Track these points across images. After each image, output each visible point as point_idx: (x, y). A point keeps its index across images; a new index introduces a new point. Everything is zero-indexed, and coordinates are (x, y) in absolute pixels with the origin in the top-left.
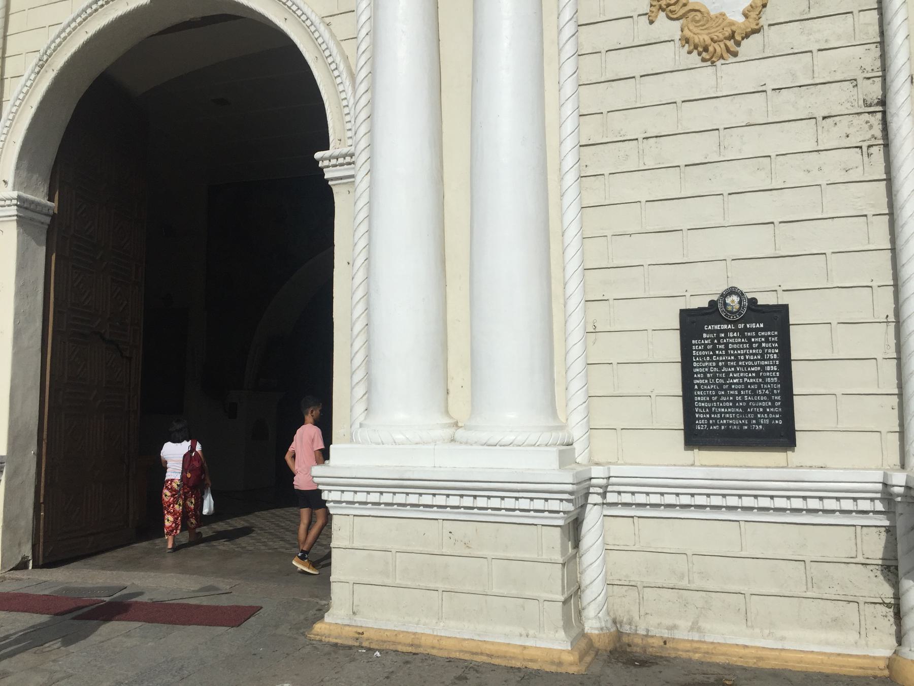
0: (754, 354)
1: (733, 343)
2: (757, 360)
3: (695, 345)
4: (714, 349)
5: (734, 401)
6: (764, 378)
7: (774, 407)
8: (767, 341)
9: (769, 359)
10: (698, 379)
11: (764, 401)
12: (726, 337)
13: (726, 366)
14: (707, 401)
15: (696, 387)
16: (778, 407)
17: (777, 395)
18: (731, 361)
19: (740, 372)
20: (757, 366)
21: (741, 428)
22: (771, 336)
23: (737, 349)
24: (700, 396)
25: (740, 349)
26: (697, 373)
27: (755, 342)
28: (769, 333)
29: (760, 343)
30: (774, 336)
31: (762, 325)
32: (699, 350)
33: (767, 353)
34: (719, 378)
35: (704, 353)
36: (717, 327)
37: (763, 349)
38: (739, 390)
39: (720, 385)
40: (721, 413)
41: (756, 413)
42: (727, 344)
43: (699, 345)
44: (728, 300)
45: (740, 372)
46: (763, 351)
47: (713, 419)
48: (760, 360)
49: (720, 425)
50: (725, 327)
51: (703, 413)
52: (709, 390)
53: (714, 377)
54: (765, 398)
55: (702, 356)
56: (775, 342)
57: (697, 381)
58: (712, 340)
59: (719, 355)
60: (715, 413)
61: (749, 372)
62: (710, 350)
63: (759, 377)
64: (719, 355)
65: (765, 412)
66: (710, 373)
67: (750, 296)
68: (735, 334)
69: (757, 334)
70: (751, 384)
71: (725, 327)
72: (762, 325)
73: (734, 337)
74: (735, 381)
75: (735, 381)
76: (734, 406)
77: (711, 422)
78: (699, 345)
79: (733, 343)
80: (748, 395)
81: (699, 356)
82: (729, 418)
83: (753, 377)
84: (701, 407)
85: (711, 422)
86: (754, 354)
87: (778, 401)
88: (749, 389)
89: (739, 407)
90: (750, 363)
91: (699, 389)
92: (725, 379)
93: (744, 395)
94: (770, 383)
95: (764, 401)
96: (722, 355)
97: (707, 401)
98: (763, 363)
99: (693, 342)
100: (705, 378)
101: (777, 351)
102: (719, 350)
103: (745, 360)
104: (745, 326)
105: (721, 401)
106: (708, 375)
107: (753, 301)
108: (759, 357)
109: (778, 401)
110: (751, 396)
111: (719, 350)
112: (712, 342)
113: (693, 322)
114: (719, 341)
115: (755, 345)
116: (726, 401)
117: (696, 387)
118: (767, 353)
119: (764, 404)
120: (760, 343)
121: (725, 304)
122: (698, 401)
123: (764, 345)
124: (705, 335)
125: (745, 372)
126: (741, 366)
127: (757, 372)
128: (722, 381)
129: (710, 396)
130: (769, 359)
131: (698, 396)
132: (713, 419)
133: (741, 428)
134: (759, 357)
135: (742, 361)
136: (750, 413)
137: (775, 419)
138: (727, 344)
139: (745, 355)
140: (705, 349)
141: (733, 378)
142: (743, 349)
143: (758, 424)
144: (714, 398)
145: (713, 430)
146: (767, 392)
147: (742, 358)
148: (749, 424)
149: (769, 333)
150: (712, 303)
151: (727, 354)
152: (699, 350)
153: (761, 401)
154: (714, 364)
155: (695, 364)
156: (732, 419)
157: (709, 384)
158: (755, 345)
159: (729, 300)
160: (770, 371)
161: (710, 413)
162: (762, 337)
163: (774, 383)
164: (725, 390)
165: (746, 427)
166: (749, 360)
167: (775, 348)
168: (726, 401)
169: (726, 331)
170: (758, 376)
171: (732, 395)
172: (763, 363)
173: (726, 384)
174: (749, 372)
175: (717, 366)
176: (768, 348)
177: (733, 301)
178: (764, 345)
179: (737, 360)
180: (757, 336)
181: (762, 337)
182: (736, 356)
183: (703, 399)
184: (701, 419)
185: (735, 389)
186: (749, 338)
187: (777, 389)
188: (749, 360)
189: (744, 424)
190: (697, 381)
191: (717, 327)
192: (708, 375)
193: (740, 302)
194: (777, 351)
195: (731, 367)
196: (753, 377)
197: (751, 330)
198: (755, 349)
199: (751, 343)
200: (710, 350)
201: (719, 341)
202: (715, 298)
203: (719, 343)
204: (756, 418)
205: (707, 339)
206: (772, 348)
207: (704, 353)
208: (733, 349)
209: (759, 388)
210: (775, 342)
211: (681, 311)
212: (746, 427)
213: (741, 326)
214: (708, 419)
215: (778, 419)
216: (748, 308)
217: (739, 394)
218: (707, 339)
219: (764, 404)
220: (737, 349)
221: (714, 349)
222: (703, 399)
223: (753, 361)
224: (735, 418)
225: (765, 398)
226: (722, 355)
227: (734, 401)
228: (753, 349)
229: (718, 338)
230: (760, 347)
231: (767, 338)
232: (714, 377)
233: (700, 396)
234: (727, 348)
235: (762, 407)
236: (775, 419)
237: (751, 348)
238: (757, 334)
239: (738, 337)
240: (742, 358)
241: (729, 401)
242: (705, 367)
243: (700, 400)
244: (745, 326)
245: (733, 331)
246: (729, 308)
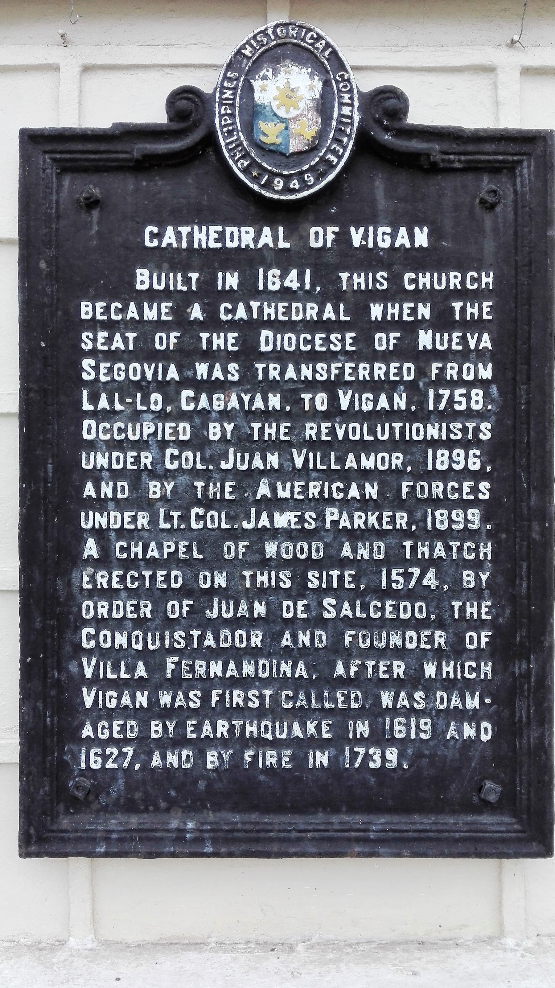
0: (375, 386)
1: (276, 326)
2: (391, 415)
3: (93, 324)
4: (186, 355)
5: (273, 624)
6: (414, 505)
7: (457, 651)
8: (442, 321)
9: (449, 415)
10: (100, 504)
11: (417, 625)
12: (249, 291)
13: (244, 443)
14: (140, 623)
15: (91, 548)
16: (478, 655)
17: (477, 594)
18: (266, 415)
19: (304, 473)
20: (393, 445)
21: (299, 760)
22: (462, 294)
23: (298, 358)
24: (109, 594)
25: (313, 357)
26: (96, 475)
27: (385, 325)
28: (454, 280)
29: (410, 329)
30: (477, 296)
31: (422, 238)
32: (113, 356)
33: (441, 381)
34: (208, 503)
35: (136, 371)
36: (206, 237)
37: (423, 358)
38: (299, 567)
39: (210, 541)
40: (207, 684)
41: (372, 686)
42: (249, 329)
43: (111, 326)
44: (268, 89)
45: (304, 473)
46: (422, 372)
47: (166, 714)
48: (408, 416)
49: (201, 746)
50: (243, 236)
51: (118, 685)
52: (153, 564)
53: (183, 500)
54: (420, 609)
55: (127, 388)
56: (477, 325)
57: (100, 520)
58: (182, 301)
59: (211, 386)
60: (176, 683)
61: (346, 476)
62: (165, 356)
63: (398, 503)
64: (211, 386)
65: (415, 680)
66: (167, 475)
67: (367, 83)
68: (292, 281)
69: (395, 280)
70: (355, 536)
71: (243, 236)
72: (422, 238)
73: (285, 293)
74: (284, 520)
75: (284, 520)
76: (271, 650)
77: (156, 729)
78: (111, 326)
79: (276, 326)
80: (339, 593)
81: (112, 388)
82: (242, 711)
83: (364, 504)
84: (113, 655)
85: (156, 729)
86: (375, 386)
87: (478, 625)
88: (344, 564)
89: (293, 654)
90: (357, 431)
91: (105, 561)
92: (237, 508)
93: (321, 592)
94: (445, 536)
95: (417, 625)
96: (222, 386)
97: (140, 623)
98: (416, 432)
99: (86, 310)
100: (139, 501)
101: (486, 373)
102: (210, 356)
103: (334, 412)
104: (343, 238)
105: (206, 625)
106: (154, 489)
107: (386, 105)
108: (400, 402)
109: (478, 625)
110: (354, 595)
111: (210, 356)
112: (180, 321)
113: (92, 204)
114: (212, 313)
115: (383, 341)
116: (235, 623)
117: (91, 548)
118: (441, 381)
119: (412, 640)
120: (410, 329)
121: (252, 113)
122: (100, 623)
123: (425, 339)
124: (143, 278)
125: (329, 475)
126: (313, 445)
127: (387, 478)
128: (217, 520)
129: (160, 597)
130: (449, 415)
131: (97, 593)
132: (166, 714)
133: (299, 760)
134: (400, 402)
135: (315, 415)
136: (346, 682)
137: (462, 715)
138: (249, 329)
139: (331, 387)
140: (145, 353)
141: (274, 504)
142: (329, 356)
143: (380, 738)
144: (177, 609)
145: (168, 771)
146: (430, 580)
147: (321, 402)
148: (340, 740)
149: (454, 280)
150: (187, 105)
151: (249, 382)
152: (113, 356)
153: (402, 625)
154: (185, 431)
155: (89, 429)
156: (260, 714)
157: (155, 533)
158: (383, 341)
159: (268, 89)
160: (445, 476)
161: (154, 683)
162: (418, 295)
163: (467, 534)
164: (233, 567)
165: (323, 758)
166: (352, 415)
167: (480, 355)
168: (235, 623)
169: (247, 261)
170: (391, 499)
171: (261, 593)
172: (416, 432)
173: (235, 535)
174: (346, 476)
175: (199, 442)
176: (444, 356)
177: (290, 94)
178: (425, 339)
179: (295, 414)
180: (396, 293)
181: (418, 295)
182: (291, 392)
183: (124, 608)
184: (111, 715)
185: (280, 563)
186: (360, 301)
187: (477, 565)
188: (352, 415)
189: (318, 743)
190: (100, 520)
191: (206, 237)
192: (154, 489)
193: (323, 107)
194: (486, 373)
195: (266, 446)
196: (364, 504)
197: (369, 259)
198: (386, 357)
199: (365, 329)
200: (165, 356)
201: (212, 313)
202: (206, 83)
203: (213, 323)
204: (374, 712)
205: (151, 295)
206: (464, 355)
207: (136, 371)
208: (280, 356)
209: (394, 559)
210: (477, 325)
211: (31, 140)
212: (323, 758)
213: (321, 236)
214: (144, 716)
215: (474, 717)
216: (366, 145)
217: (300, 590)
218: (151, 295)
219: (412, 640)
220: (298, 358)
221: (186, 355)
222: (124, 608)
223: (374, 417)
224: (274, 712)
225: (420, 609)
226: (222, 386)
227: (273, 624)
228: (374, 357)
229: (210, 295)
230: (406, 351)
231: (441, 300)
232: (183, 500)
233: (109, 594)
234: (248, 353)
235: (400, 653)
236: (462, 715)
237: (366, 353)
238: (395, 280)
239: (305, 296)
240: (321, 402)
241: (251, 622)
242: (140, 445)
243: (108, 617)
244: (343, 238)
245: (283, 260)
246: (269, 132)
